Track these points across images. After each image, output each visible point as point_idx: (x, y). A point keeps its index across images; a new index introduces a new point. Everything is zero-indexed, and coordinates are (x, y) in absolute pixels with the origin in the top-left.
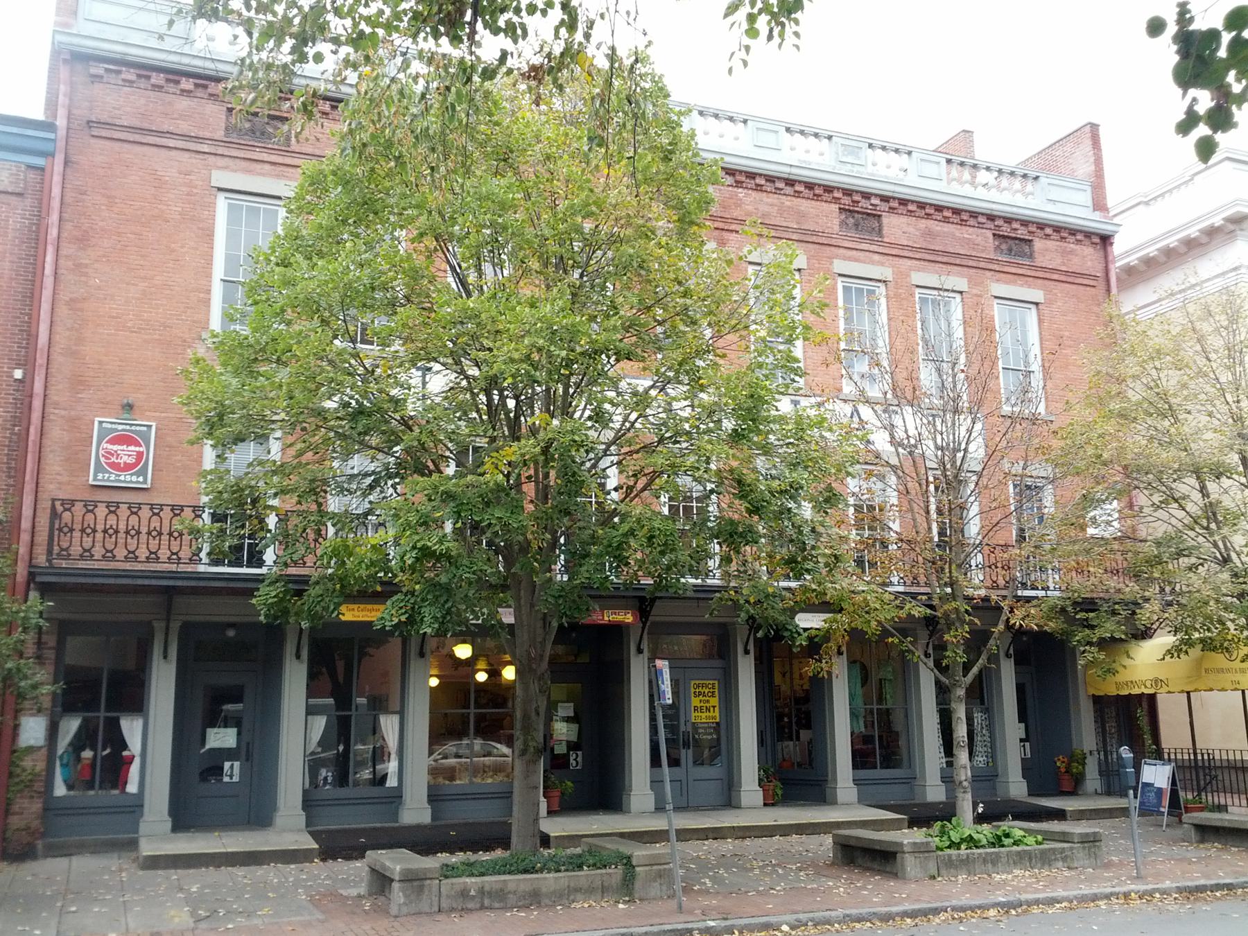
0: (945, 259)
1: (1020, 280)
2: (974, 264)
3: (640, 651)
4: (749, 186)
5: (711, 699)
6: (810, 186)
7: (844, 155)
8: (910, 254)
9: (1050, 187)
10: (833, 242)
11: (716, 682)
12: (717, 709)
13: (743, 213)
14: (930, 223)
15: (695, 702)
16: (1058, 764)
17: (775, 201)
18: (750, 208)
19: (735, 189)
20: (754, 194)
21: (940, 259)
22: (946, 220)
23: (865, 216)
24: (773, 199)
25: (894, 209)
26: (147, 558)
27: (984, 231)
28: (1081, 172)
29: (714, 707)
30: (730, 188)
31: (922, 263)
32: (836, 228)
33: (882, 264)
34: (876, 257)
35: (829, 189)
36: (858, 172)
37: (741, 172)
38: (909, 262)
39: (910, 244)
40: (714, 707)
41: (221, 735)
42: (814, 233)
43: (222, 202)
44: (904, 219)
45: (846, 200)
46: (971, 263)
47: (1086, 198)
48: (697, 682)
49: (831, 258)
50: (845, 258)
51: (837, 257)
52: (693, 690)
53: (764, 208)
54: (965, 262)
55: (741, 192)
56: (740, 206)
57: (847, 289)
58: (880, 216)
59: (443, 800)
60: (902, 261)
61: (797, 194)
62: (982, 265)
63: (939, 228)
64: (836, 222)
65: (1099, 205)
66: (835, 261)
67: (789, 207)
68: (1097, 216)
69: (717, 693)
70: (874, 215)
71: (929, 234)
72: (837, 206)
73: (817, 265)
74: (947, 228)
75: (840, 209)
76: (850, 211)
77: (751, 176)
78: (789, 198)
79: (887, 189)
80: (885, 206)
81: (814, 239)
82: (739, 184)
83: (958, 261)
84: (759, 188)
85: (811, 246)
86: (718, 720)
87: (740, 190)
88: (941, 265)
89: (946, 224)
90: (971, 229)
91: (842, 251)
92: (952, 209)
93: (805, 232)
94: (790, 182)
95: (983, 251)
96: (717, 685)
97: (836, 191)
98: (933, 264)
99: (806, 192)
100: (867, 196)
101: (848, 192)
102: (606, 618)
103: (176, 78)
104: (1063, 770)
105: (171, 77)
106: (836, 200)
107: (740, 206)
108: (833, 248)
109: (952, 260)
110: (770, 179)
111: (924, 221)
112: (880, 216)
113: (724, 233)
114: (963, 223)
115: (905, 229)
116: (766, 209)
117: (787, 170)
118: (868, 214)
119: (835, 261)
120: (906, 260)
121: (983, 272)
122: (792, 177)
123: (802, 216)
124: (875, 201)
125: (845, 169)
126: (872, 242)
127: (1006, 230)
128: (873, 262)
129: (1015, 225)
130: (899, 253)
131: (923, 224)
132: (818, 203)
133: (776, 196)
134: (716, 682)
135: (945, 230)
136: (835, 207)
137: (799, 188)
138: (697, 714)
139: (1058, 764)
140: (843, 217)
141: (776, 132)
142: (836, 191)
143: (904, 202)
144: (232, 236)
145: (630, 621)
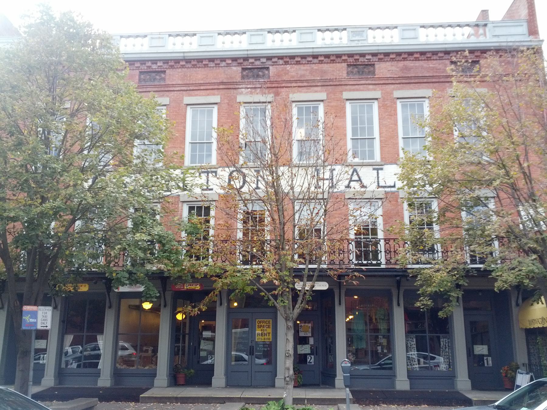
0: (416, 81)
1: (305, 89)
2: (437, 80)
3: (110, 307)
4: (411, 59)
5: (268, 329)
6: (327, 56)
7: (353, 36)
8: (393, 82)
9: (203, 39)
10: (343, 83)
11: (271, 320)
12: (271, 335)
13: (290, 77)
14: (407, 63)
15: (258, 331)
16: (501, 371)
17: (308, 68)
18: (293, 74)
19: (285, 66)
20: (296, 66)
21: (413, 81)
22: (417, 59)
23: (364, 66)
24: (307, 67)
25: (382, 59)
26: (114, 265)
27: (444, 61)
28: (523, 15)
29: (269, 333)
30: (282, 66)
31: (402, 85)
32: (345, 75)
33: (375, 90)
34: (371, 87)
35: (339, 56)
36: (361, 44)
37: (286, 56)
38: (393, 86)
39: (392, 76)
40: (269, 333)
41: (40, 343)
42: (331, 80)
43: (189, 112)
44: (389, 64)
45: (351, 60)
46: (434, 80)
47: (524, 29)
48: (260, 320)
49: (341, 92)
50: (350, 90)
51: (346, 90)
52: (257, 324)
53: (301, 72)
54: (430, 80)
55: (288, 67)
56: (288, 74)
57: (300, 110)
58: (374, 65)
59: (124, 376)
60: (387, 86)
61: (321, 62)
62: (442, 80)
63: (412, 65)
64: (345, 72)
65: (533, 31)
66: (344, 93)
67: (316, 70)
68: (531, 38)
69: (271, 326)
70: (370, 65)
71: (406, 68)
72: (346, 64)
73: (333, 97)
74: (417, 63)
75: (348, 65)
76: (355, 65)
77: (292, 57)
78: (317, 65)
79: (374, 49)
80: (375, 59)
81: (331, 83)
82: (286, 63)
83: (425, 81)
84: (298, 63)
85: (330, 87)
86: (271, 340)
87: (288, 66)
88: (414, 85)
89: (417, 62)
90: (435, 62)
91: (348, 87)
92: (208, 59)
93: (326, 80)
94: (315, 57)
95: (443, 72)
96: (271, 322)
97: (215, 60)
98: (409, 85)
99: (326, 60)
100: (363, 55)
101: (351, 55)
102: (185, 288)
103: (155, 62)
104: (504, 375)
105: (153, 62)
106: (345, 61)
107: (288, 74)
108: (343, 87)
109: (421, 81)
110: (304, 57)
111: (402, 62)
112: (268, 68)
113: (279, 89)
114: (428, 59)
115: (390, 69)
116: (303, 73)
117: (246, 53)
118: (367, 65)
119: (344, 93)
120: (390, 85)
121: (443, 84)
122: (314, 54)
123: (324, 72)
124: (264, 60)
125: (353, 44)
126: (367, 79)
127: (246, 65)
128: (369, 90)
129: (160, 64)
130: (386, 82)
131: (401, 64)
132: (334, 64)
133: (308, 65)
134: (271, 320)
135: (417, 64)
136: (344, 64)
137: (321, 58)
138: (259, 337)
139: (501, 371)
140: (349, 69)
141: (415, 29)
142: (367, 55)
143: (387, 54)
144: (194, 123)
145: (198, 289)
